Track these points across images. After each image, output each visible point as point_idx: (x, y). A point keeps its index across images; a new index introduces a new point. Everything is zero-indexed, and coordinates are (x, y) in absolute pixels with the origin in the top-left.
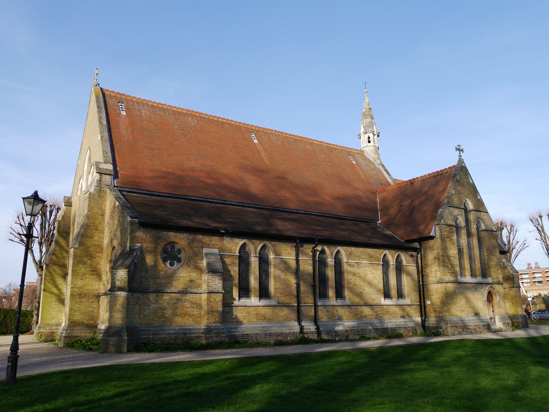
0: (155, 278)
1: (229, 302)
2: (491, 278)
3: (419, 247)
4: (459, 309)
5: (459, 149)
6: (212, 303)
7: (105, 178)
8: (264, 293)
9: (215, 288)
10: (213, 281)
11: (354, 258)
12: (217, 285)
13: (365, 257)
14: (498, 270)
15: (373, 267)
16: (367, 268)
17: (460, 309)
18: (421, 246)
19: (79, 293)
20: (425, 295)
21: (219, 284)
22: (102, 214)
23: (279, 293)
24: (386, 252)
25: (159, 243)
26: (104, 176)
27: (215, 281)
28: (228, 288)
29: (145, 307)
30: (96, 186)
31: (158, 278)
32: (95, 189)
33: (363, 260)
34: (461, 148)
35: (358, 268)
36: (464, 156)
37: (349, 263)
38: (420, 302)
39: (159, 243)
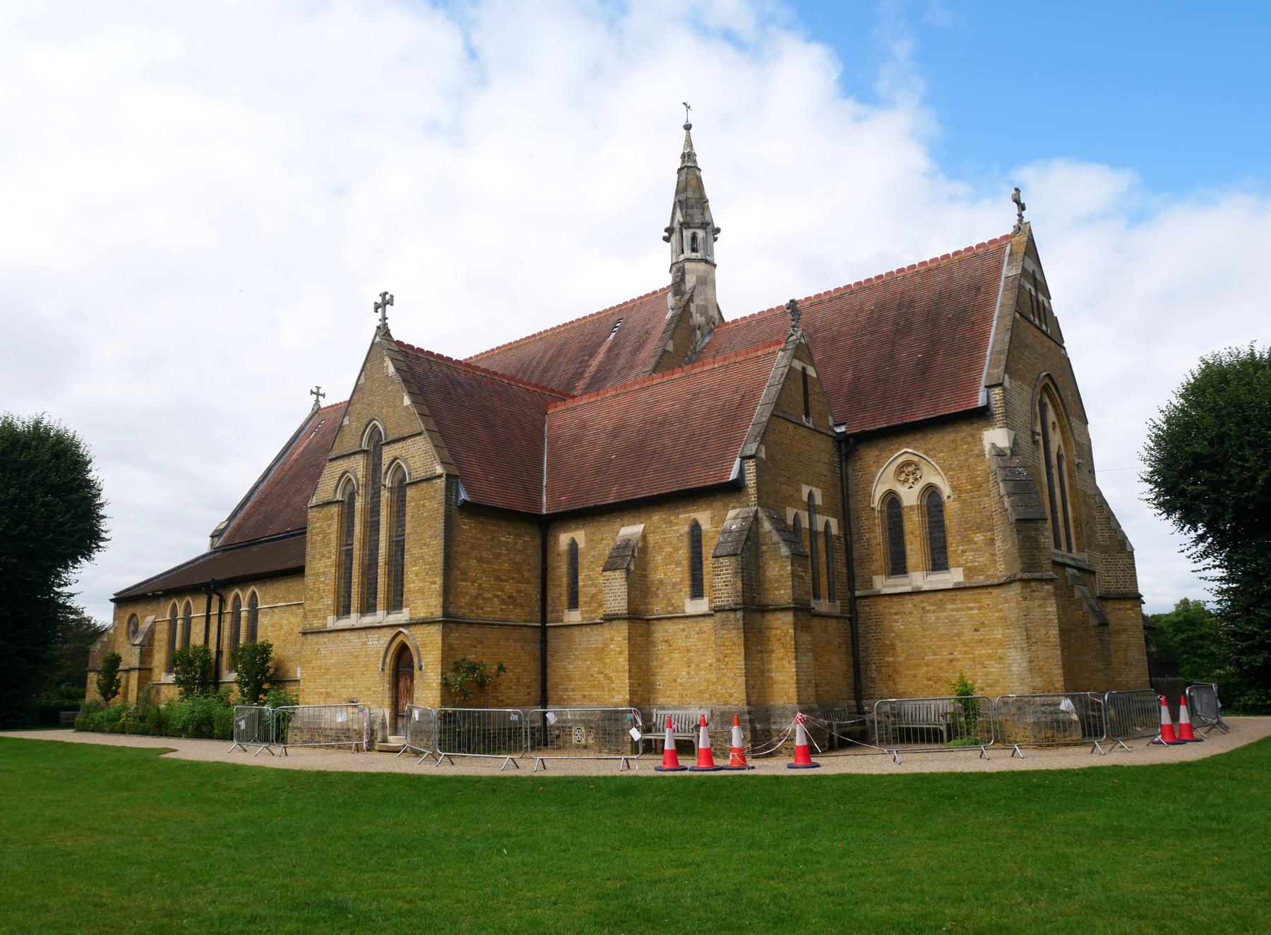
4: (321, 690)
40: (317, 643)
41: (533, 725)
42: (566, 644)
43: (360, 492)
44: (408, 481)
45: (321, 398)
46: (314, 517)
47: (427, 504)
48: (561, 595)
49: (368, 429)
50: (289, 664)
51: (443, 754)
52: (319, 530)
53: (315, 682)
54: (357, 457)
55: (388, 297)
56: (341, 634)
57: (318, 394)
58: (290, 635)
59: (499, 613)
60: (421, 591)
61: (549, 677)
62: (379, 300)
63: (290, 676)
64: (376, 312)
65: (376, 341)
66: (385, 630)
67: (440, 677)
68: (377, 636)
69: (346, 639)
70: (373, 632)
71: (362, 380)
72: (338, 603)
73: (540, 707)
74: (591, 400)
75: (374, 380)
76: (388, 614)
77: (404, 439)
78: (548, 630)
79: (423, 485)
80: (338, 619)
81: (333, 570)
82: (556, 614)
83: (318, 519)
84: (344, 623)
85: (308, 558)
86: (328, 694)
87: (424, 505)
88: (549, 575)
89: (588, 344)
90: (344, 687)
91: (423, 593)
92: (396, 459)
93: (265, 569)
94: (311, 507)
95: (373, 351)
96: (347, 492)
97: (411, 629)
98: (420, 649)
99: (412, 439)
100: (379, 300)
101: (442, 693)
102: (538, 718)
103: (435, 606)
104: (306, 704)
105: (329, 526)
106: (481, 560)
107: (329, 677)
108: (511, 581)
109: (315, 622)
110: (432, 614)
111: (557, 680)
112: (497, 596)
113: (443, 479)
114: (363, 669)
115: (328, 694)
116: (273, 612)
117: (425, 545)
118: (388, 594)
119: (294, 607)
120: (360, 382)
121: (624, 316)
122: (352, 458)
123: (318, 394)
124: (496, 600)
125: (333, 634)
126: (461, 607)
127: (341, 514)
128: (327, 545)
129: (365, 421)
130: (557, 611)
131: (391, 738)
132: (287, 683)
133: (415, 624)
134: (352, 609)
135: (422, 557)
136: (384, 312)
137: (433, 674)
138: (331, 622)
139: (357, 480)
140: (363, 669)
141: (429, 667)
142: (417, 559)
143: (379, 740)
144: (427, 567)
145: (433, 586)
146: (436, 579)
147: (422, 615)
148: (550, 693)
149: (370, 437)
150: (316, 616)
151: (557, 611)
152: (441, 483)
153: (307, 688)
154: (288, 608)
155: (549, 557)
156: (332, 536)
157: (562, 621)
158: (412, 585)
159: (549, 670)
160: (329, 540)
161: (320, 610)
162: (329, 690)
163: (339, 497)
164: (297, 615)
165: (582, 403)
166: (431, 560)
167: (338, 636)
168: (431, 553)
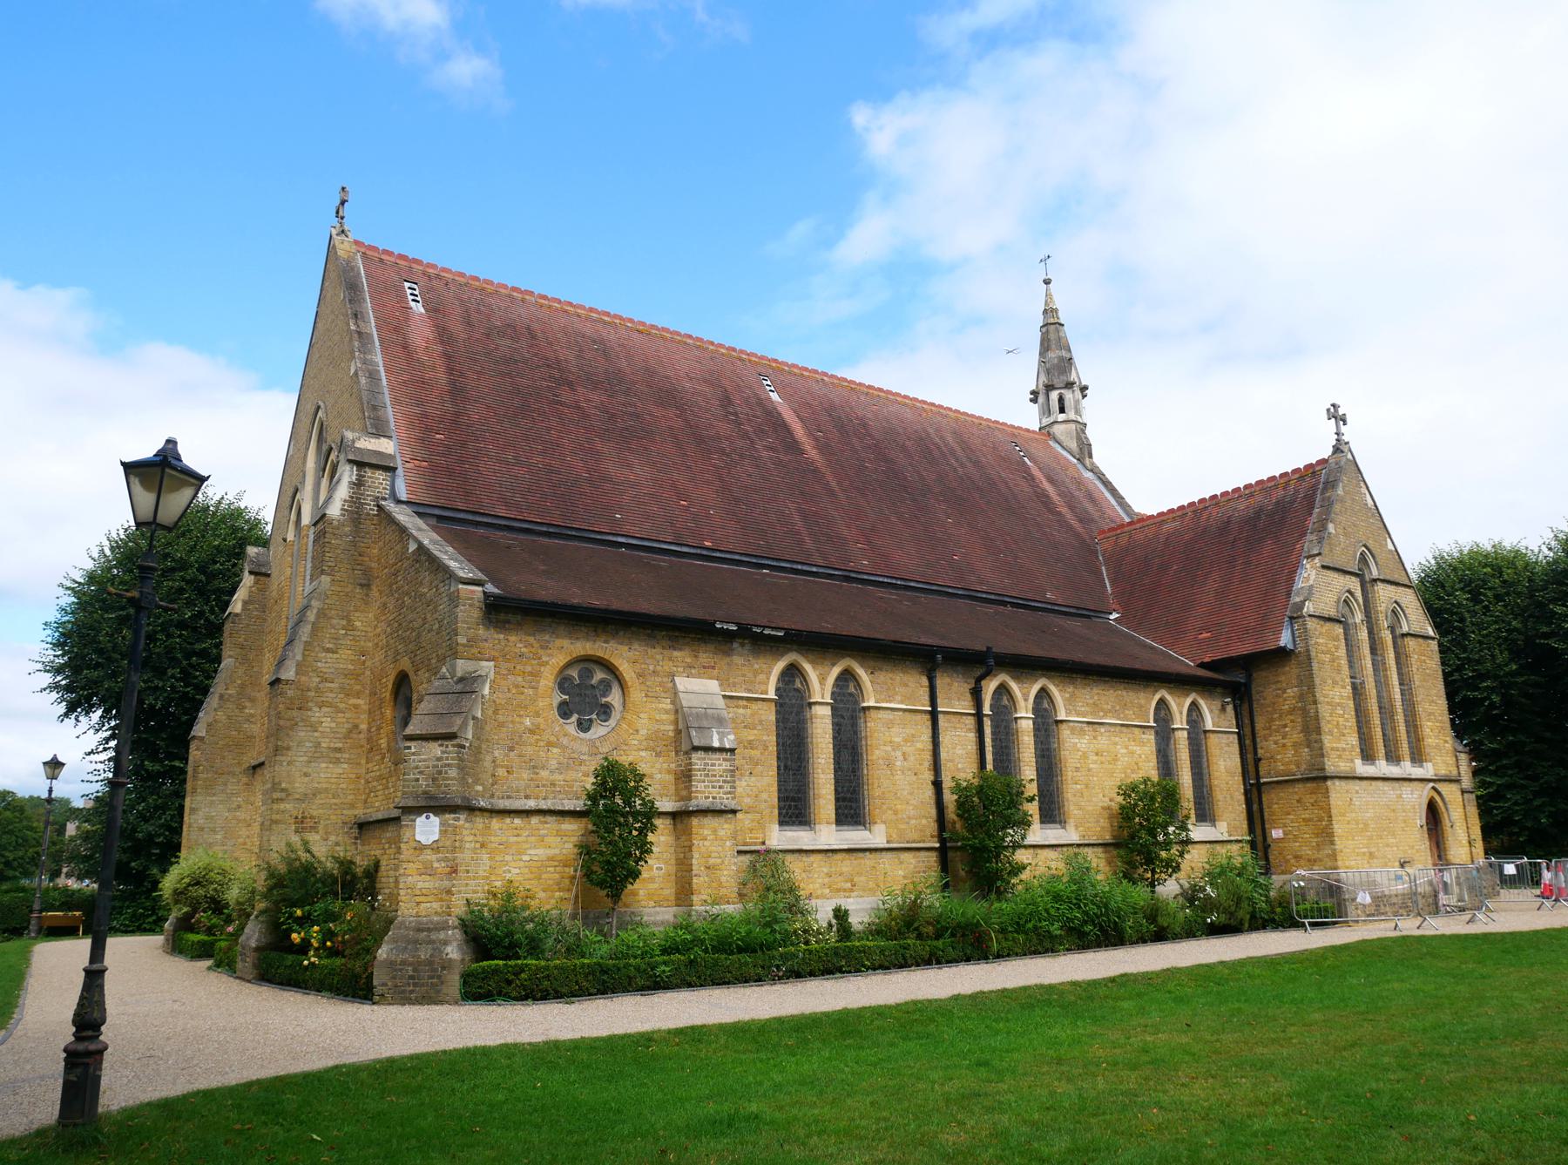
0: (534, 767)
1: (750, 838)
3: (1242, 681)
5: (1336, 415)
6: (706, 843)
7: (371, 477)
8: (851, 811)
9: (714, 798)
10: (707, 775)
11: (1083, 709)
12: (720, 787)
13: (1109, 707)
14: (1446, 742)
15: (1130, 736)
16: (1117, 739)
18: (1249, 677)
19: (296, 818)
20: (1266, 814)
21: (725, 785)
22: (364, 582)
23: (890, 812)
25: (545, 659)
26: (369, 473)
27: (715, 776)
28: (749, 796)
29: (508, 858)
30: (345, 501)
31: (543, 768)
32: (342, 509)
33: (1105, 716)
35: (1095, 738)
36: (1348, 433)
37: (1071, 724)
38: (1251, 830)
39: (545, 659)
53: (1353, 840)
56: (1374, 783)
60: (1437, 747)
62: (1341, 412)
70: (1406, 784)
79: (1420, 640)
84: (1369, 770)
90: (1388, 845)
100: (1341, 412)
104: (1347, 868)
105: (1337, 648)
116: (1095, 731)
119: (1137, 731)
128: (1339, 671)
138: (1362, 768)
140: (1403, 825)
150: (1340, 757)
154: (1124, 729)
161: (1344, 750)
164: (1142, 744)
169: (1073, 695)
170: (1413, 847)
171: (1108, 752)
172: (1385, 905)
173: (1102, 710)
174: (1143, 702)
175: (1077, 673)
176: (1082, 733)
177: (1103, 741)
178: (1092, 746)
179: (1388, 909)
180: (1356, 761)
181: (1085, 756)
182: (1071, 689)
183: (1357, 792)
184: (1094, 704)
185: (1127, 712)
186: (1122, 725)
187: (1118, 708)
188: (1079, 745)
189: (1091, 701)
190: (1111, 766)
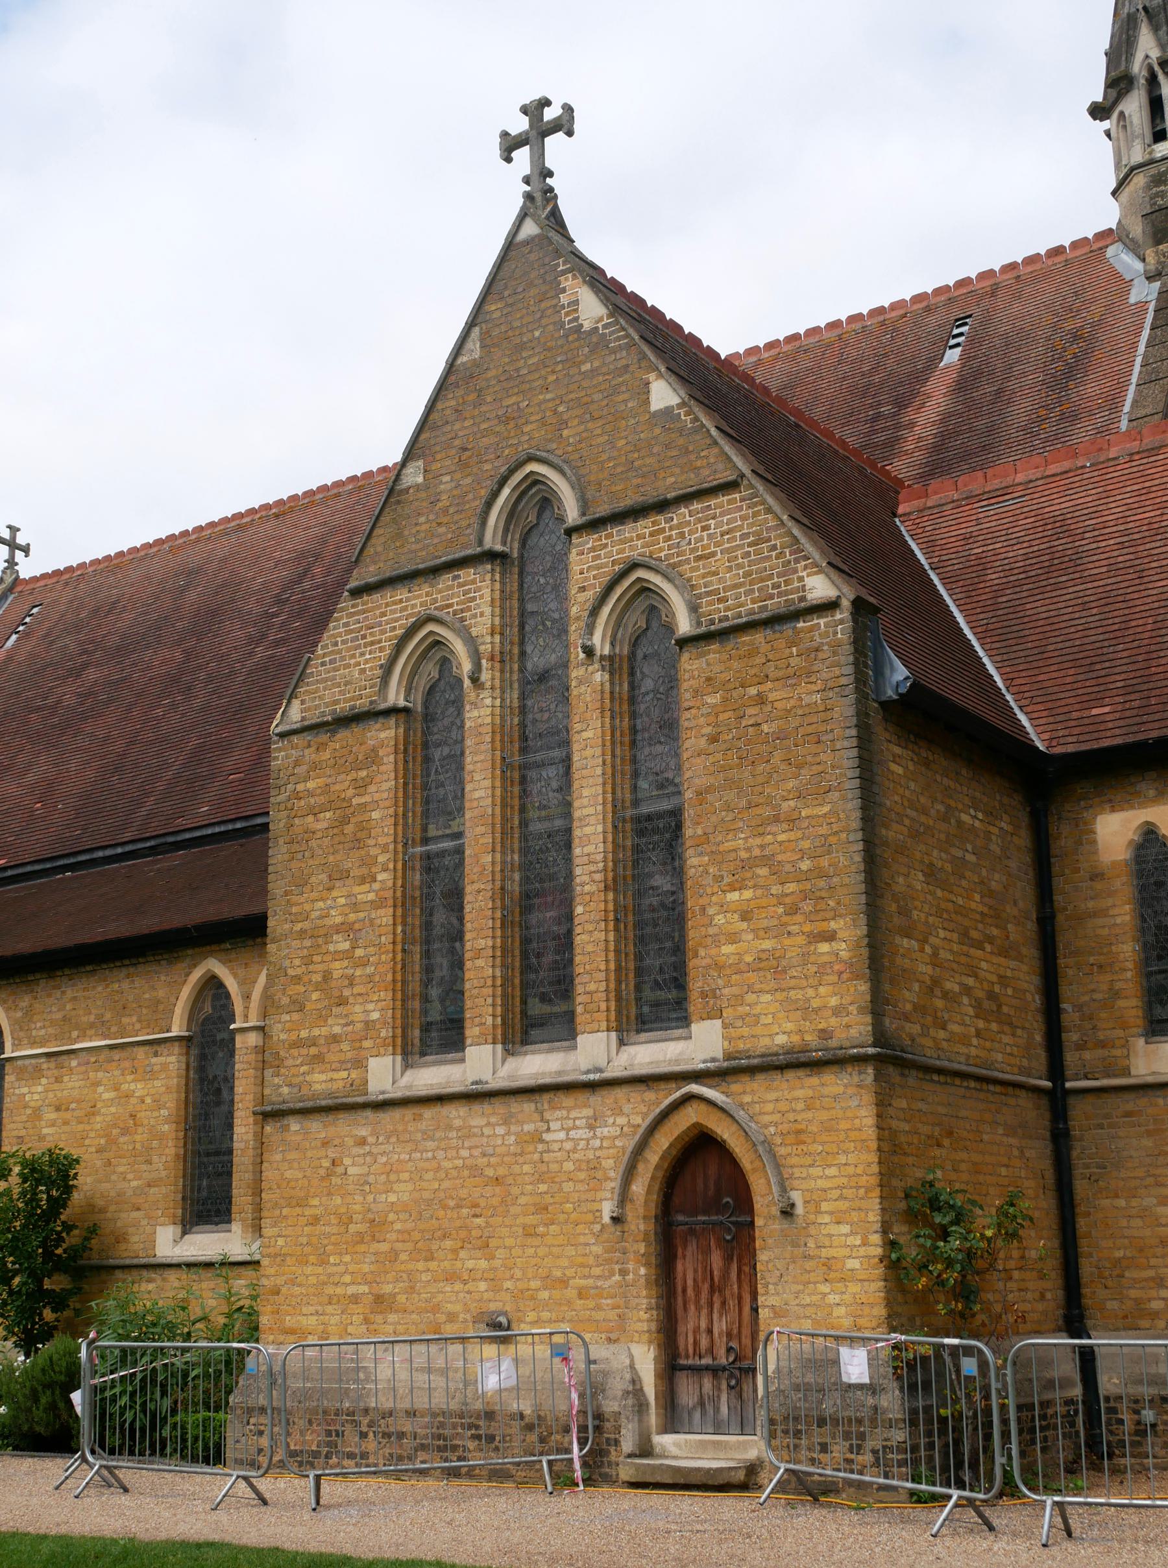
2: (718, 1023)
4: (351, 1290)
11: (42, 1032)
13: (92, 1018)
15: (127, 1064)
16: (100, 1075)
17: (364, 1289)
24: (214, 966)
33: (82, 1037)
34: (550, 114)
35: (58, 1080)
37: (20, 1063)
40: (325, 1144)
41: (1048, 1396)
42: (1147, 1142)
43: (485, 676)
44: (684, 625)
45: (19, 555)
46: (297, 763)
47: (772, 696)
48: (1116, 995)
49: (506, 491)
50: (128, 1217)
51: (955, 1494)
52: (321, 799)
53: (323, 1262)
54: (467, 574)
55: (550, 114)
56: (429, 1113)
57: (12, 545)
58: (125, 1131)
59: (975, 1041)
61: (1084, 1245)
62: (520, 125)
63: (133, 1249)
64: (508, 160)
65: (523, 235)
66: (620, 1093)
67: (876, 1238)
68: (587, 1112)
69: (450, 1127)
70: (567, 1100)
71: (474, 348)
72: (405, 1017)
73: (1064, 1334)
74: (1053, 469)
75: (521, 347)
76: (622, 1043)
77: (662, 506)
78: (1072, 1101)
80: (407, 1066)
81: (385, 916)
82: (1100, 1052)
83: (315, 766)
85: (276, 887)
86: (381, 1303)
87: (761, 700)
88: (1062, 940)
89: (876, 379)
90: (451, 1277)
91: (779, 972)
92: (634, 566)
93: (26, 944)
94: (282, 735)
95: (509, 266)
96: (422, 683)
97: (735, 1087)
98: (782, 1151)
99: (696, 506)
100: (520, 125)
101: (888, 1291)
102: (1070, 1369)
103: (837, 1011)
105: (361, 787)
106: (931, 873)
107: (384, 1247)
108: (988, 948)
109: (323, 1077)
110: (825, 1034)
111: (1119, 1254)
112: (967, 990)
113: (843, 615)
114: (531, 1220)
115: (381, 1303)
117: (776, 819)
118: (619, 982)
119: (140, 1052)
120: (460, 361)
121: (976, 311)
122: (446, 580)
123: (12, 545)
124: (965, 1000)
125: (397, 1114)
126: (906, 1018)
127: (404, 749)
128: (358, 843)
129: (493, 468)
130: (1103, 1045)
131: (666, 1441)
132: (119, 1274)
133: (752, 1071)
134: (471, 1032)
135: (766, 860)
136: (539, 156)
137: (845, 1229)
139: (472, 642)
140: (531, 1220)
141: (825, 1206)
142: (748, 865)
143: (627, 1445)
144: (791, 887)
145: (824, 947)
146: (833, 925)
147: (781, 1039)
148: (1092, 1294)
149: (512, 514)
150: (319, 1059)
151: (1103, 1045)
152: (839, 625)
153: (293, 1282)
154: (116, 1055)
155: (1058, 883)
156: (375, 815)
157: (1126, 1072)
158: (727, 949)
159: (1082, 1224)
160: (364, 828)
161: (335, 1039)
162: (387, 1289)
163: (395, 696)
164: (150, 1074)
165: (1020, 478)
166: (805, 865)
167: (418, 1118)
168: (806, 844)
169: (29, 1013)
170: (564, 1282)
171: (78, 1102)
172: (363, 1435)
173: (77, 1027)
174: (161, 993)
175: (33, 972)
176: (38, 1073)
177: (73, 1084)
178: (51, 1095)
179: (371, 1445)
180: (373, 1063)
181: (37, 1114)
182: (25, 1001)
183: (362, 1142)
184: (64, 1018)
185: (125, 1020)
186: (111, 1047)
187: (108, 1016)
188: (27, 1098)
189: (59, 1016)
190: (81, 1127)
